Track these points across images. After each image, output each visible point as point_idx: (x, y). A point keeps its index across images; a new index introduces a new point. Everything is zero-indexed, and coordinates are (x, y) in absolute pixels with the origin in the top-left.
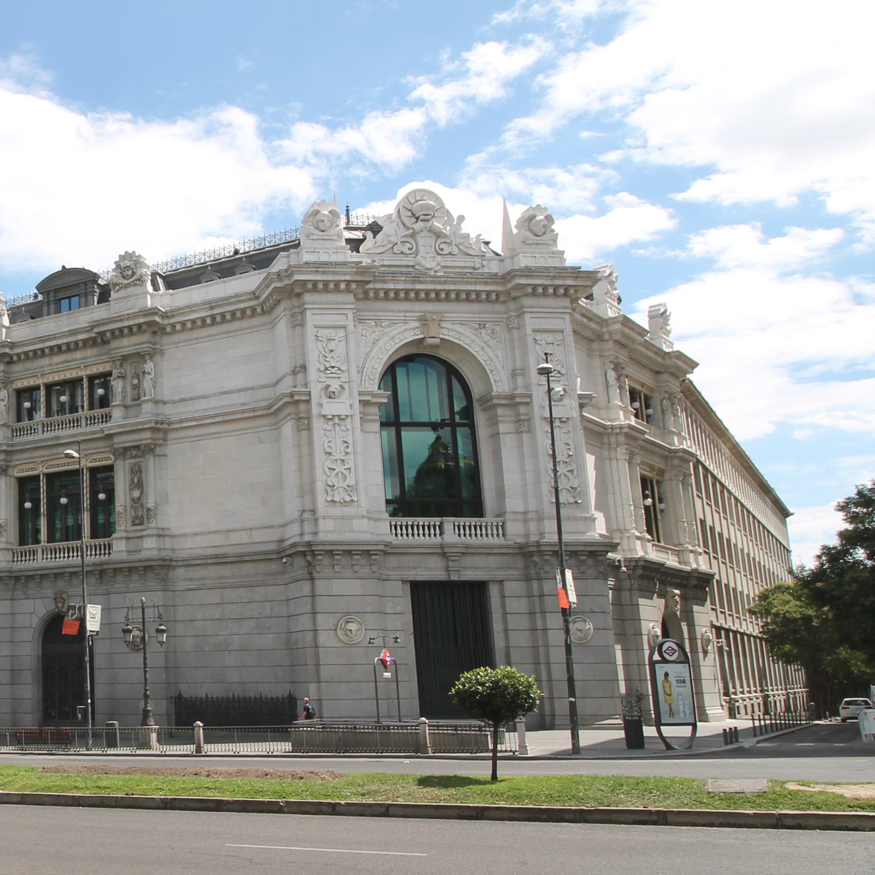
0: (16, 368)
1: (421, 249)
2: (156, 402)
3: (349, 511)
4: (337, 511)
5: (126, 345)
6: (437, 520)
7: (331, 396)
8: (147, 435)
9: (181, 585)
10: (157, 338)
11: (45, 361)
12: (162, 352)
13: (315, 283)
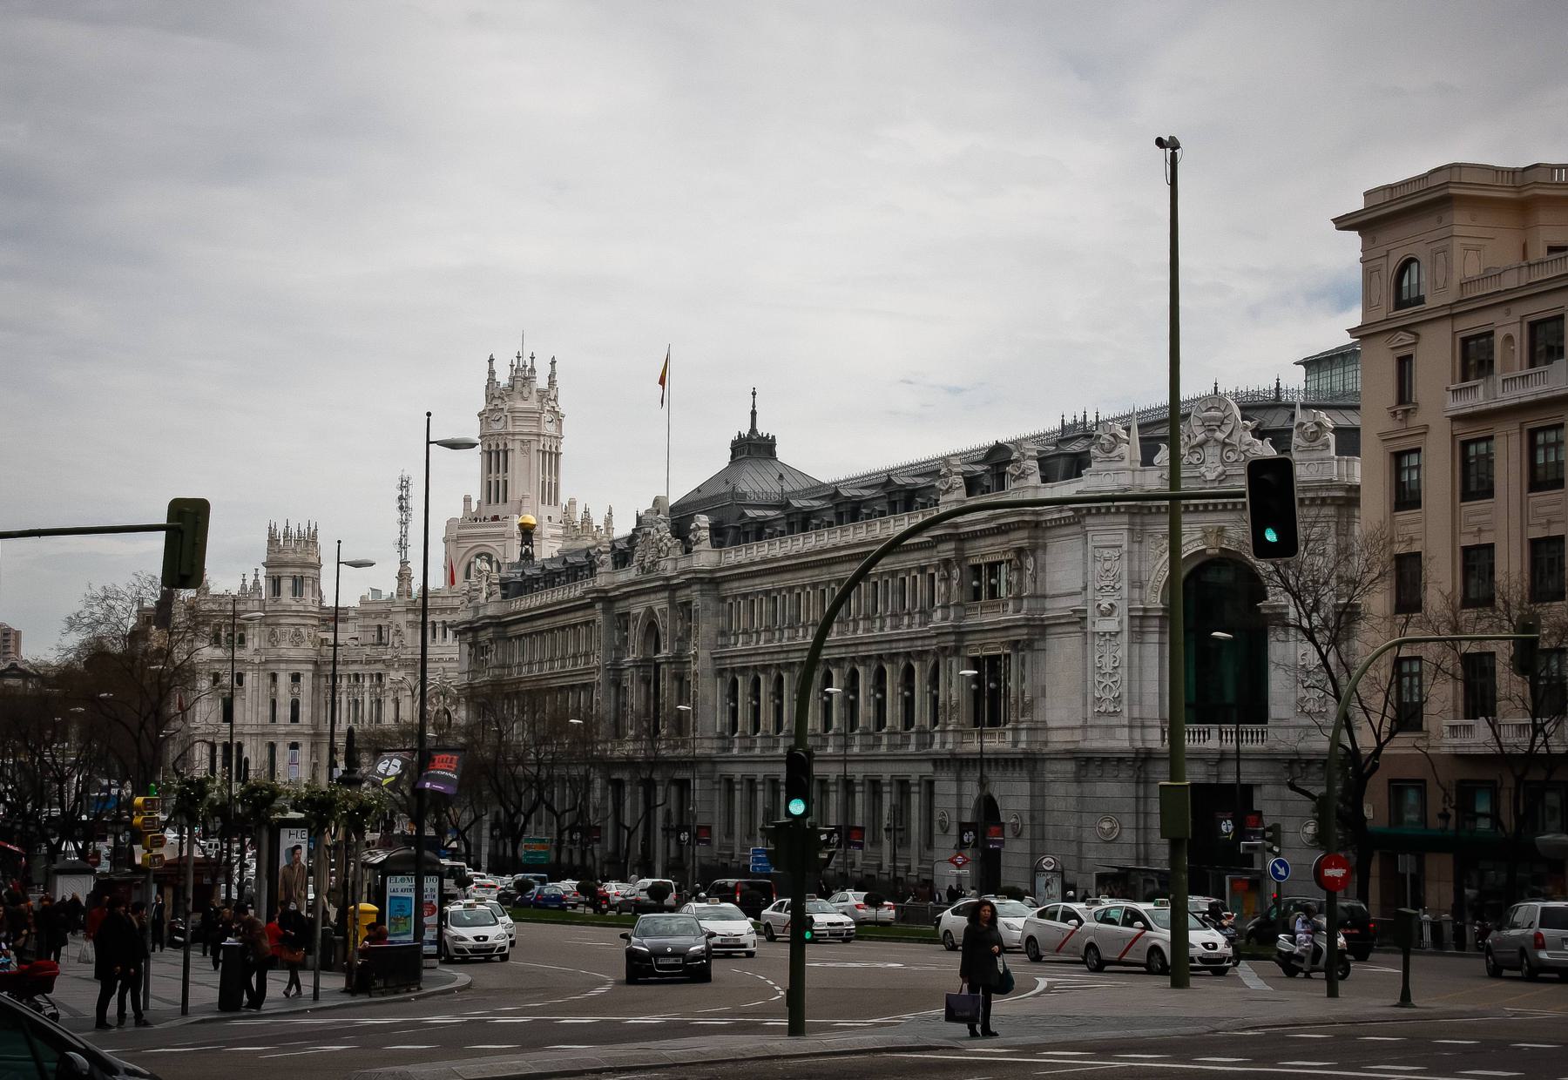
0: (968, 545)
1: (1209, 460)
2: (1034, 596)
3: (1114, 721)
4: (1103, 721)
5: (1020, 539)
6: (1205, 727)
7: (1103, 614)
8: (1025, 631)
9: (1049, 777)
10: (1040, 533)
11: (982, 543)
12: (1045, 547)
13: (1089, 509)
